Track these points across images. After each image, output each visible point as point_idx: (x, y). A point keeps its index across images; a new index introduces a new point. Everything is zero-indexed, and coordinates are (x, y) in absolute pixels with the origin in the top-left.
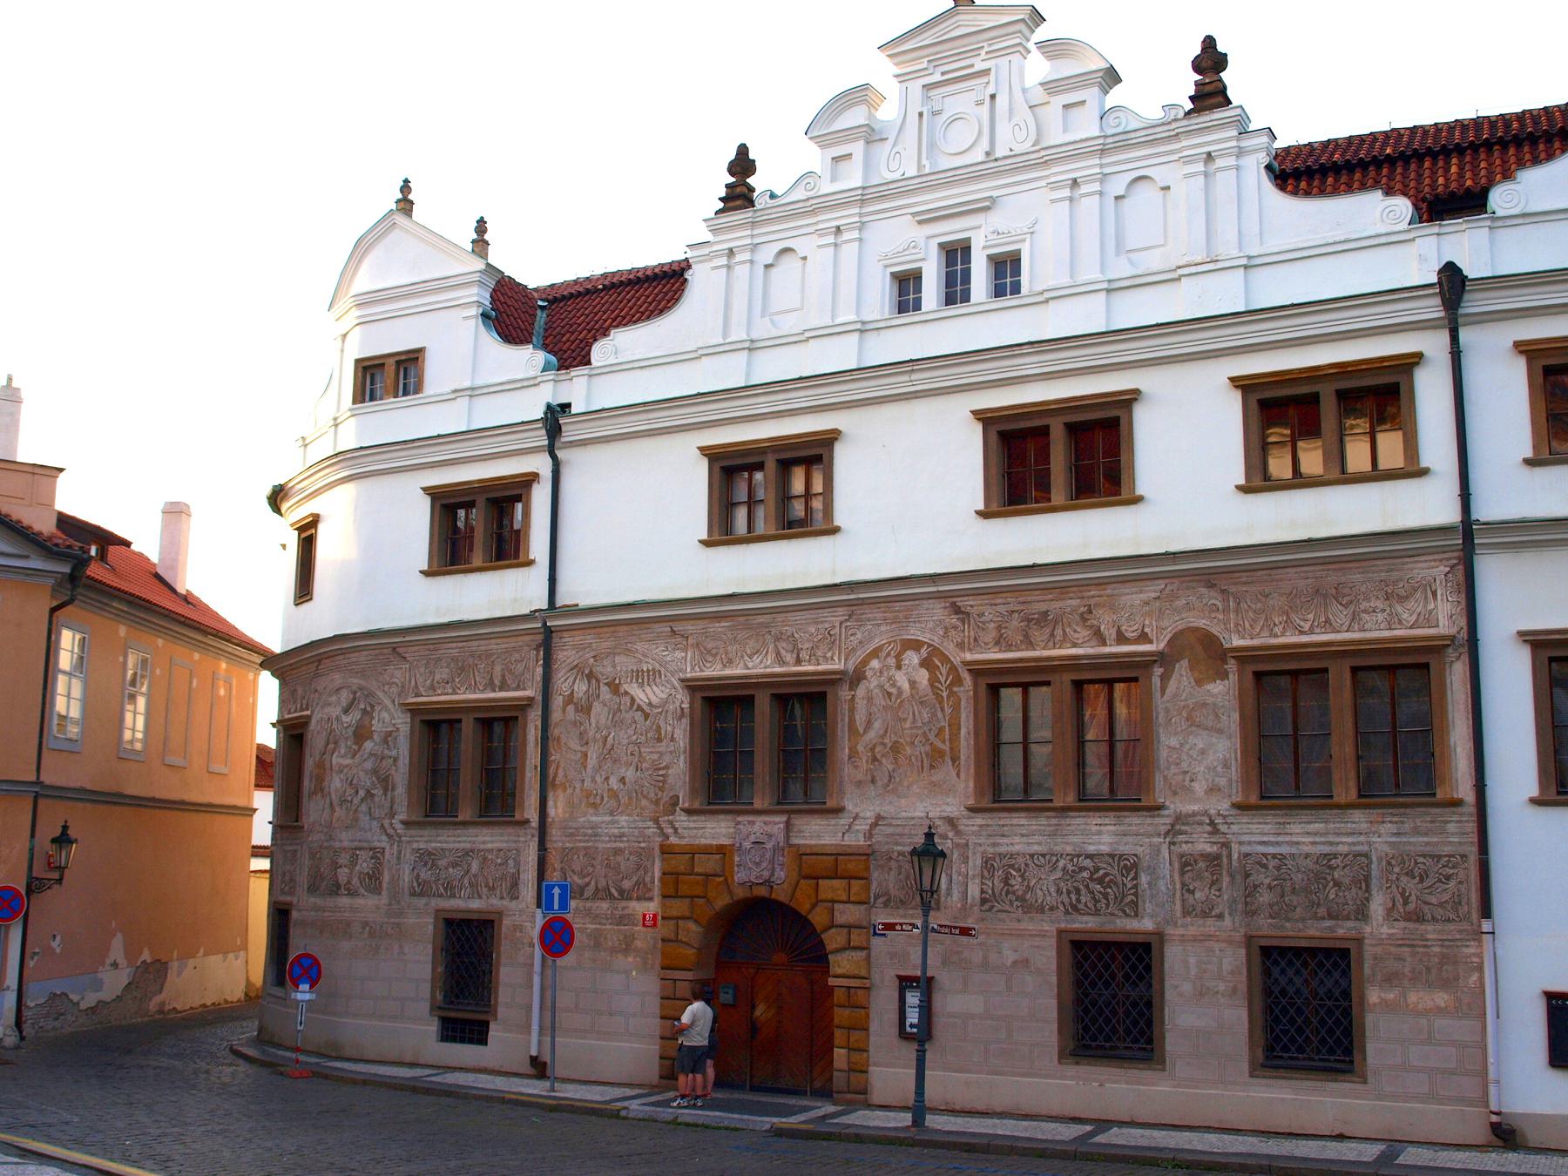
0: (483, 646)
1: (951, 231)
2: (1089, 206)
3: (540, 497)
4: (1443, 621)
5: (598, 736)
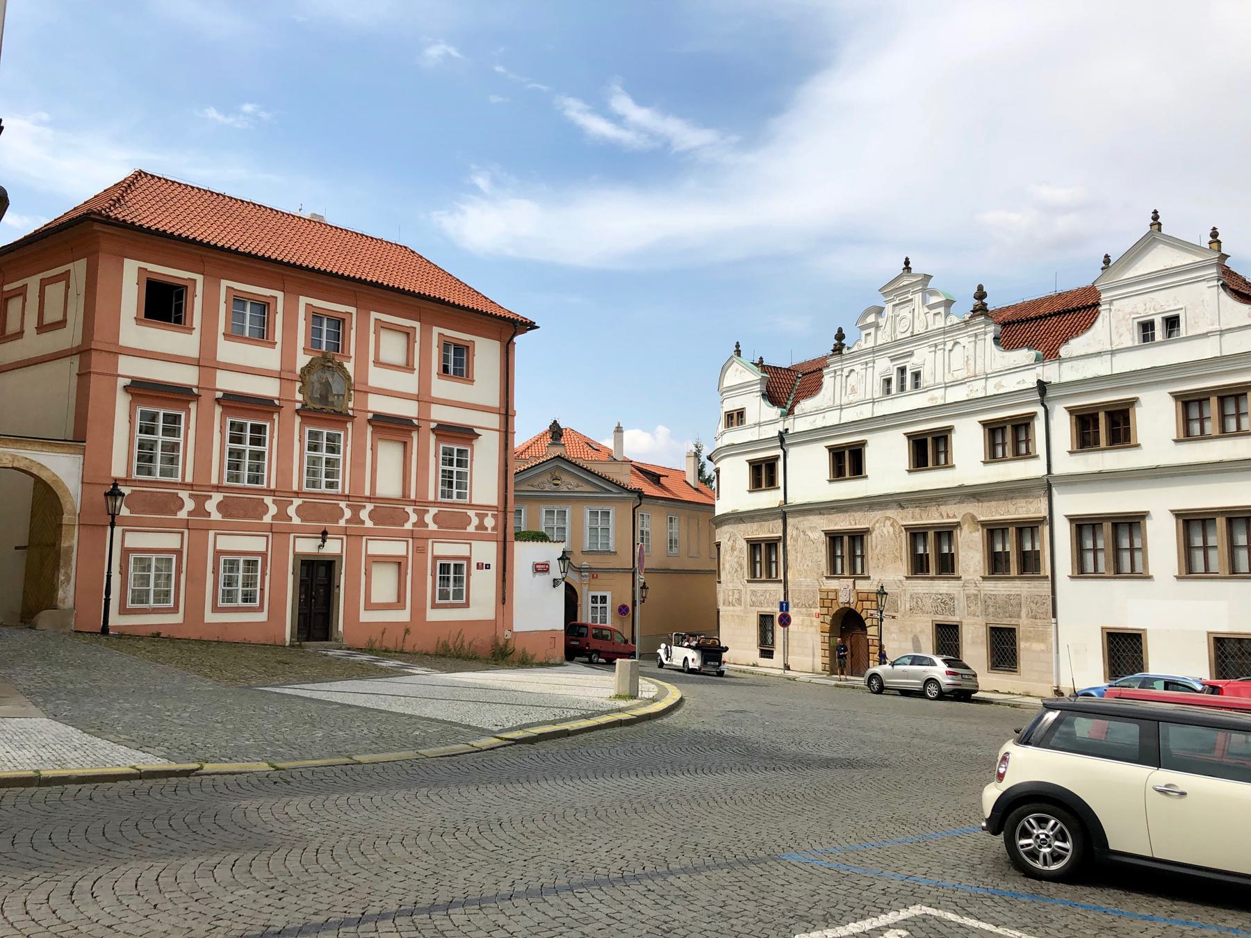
1: (900, 363)
2: (940, 353)
3: (780, 464)
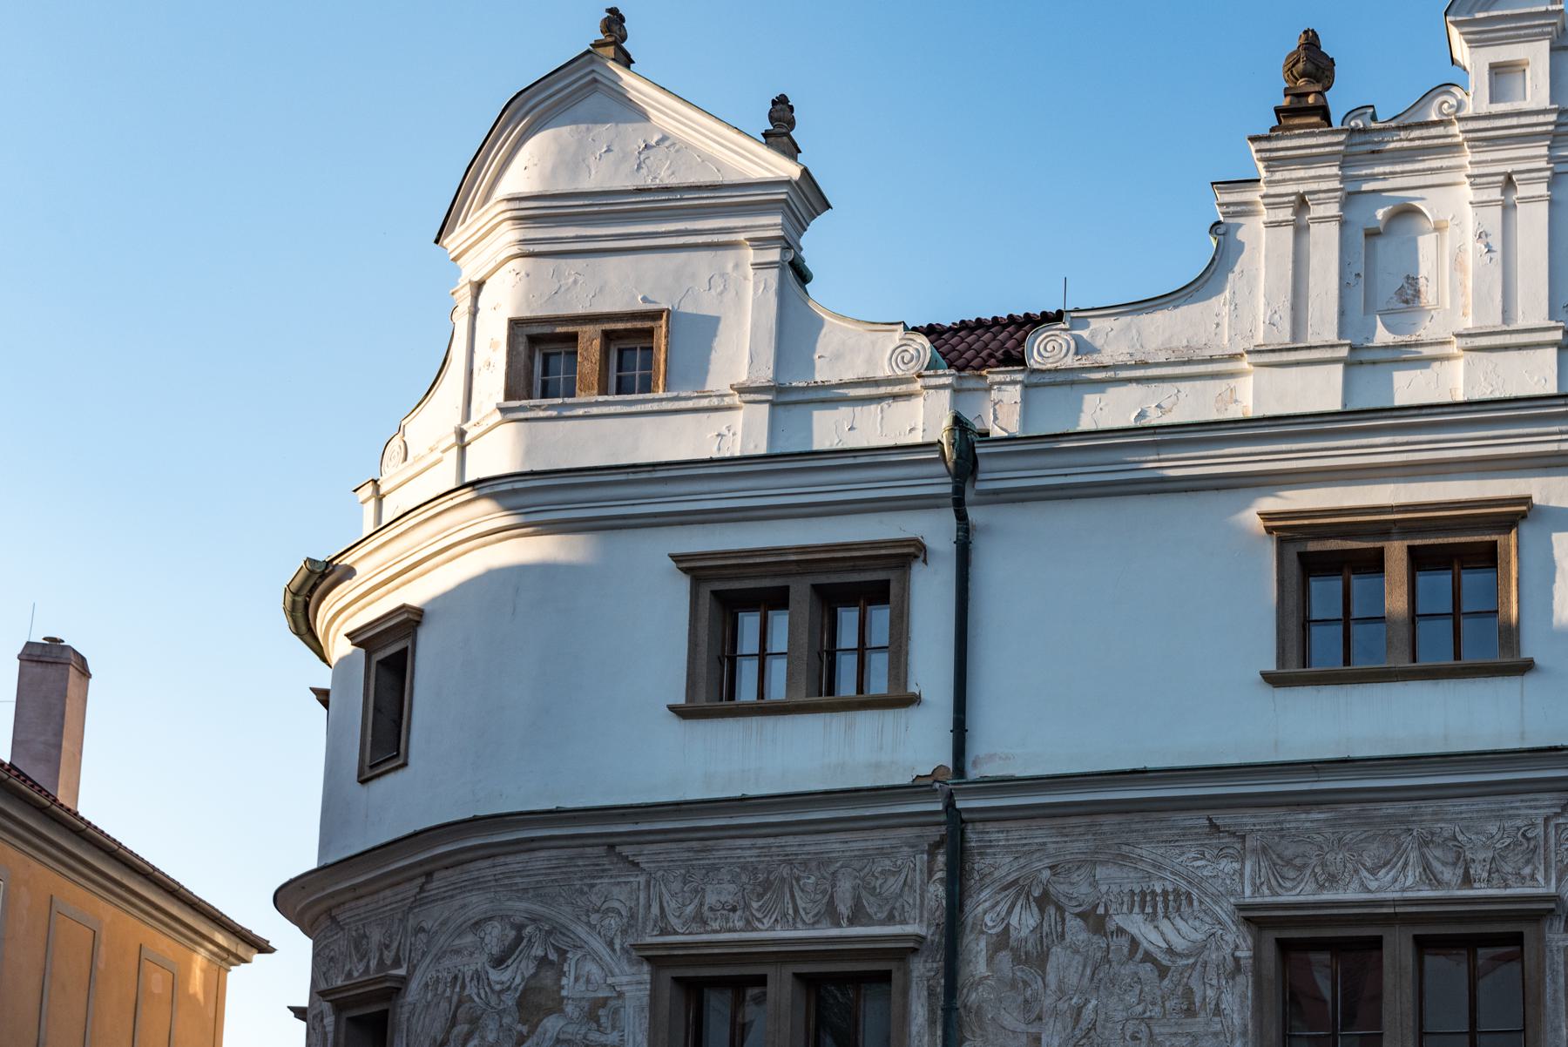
0: (812, 845)
5: (1063, 1006)
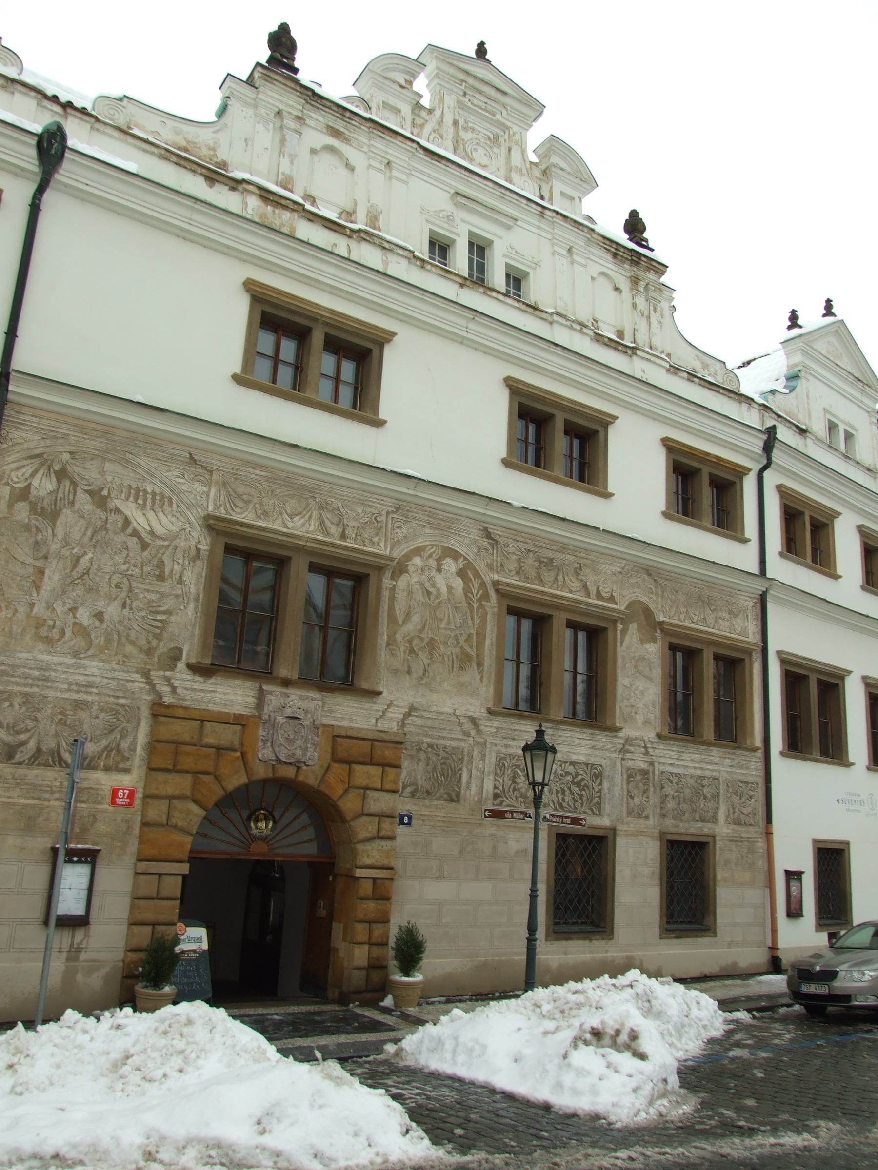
4: (751, 636)
5: (66, 552)
